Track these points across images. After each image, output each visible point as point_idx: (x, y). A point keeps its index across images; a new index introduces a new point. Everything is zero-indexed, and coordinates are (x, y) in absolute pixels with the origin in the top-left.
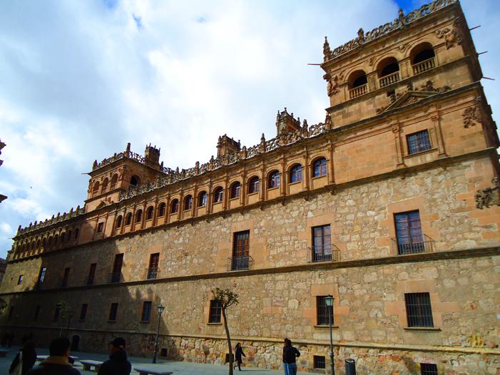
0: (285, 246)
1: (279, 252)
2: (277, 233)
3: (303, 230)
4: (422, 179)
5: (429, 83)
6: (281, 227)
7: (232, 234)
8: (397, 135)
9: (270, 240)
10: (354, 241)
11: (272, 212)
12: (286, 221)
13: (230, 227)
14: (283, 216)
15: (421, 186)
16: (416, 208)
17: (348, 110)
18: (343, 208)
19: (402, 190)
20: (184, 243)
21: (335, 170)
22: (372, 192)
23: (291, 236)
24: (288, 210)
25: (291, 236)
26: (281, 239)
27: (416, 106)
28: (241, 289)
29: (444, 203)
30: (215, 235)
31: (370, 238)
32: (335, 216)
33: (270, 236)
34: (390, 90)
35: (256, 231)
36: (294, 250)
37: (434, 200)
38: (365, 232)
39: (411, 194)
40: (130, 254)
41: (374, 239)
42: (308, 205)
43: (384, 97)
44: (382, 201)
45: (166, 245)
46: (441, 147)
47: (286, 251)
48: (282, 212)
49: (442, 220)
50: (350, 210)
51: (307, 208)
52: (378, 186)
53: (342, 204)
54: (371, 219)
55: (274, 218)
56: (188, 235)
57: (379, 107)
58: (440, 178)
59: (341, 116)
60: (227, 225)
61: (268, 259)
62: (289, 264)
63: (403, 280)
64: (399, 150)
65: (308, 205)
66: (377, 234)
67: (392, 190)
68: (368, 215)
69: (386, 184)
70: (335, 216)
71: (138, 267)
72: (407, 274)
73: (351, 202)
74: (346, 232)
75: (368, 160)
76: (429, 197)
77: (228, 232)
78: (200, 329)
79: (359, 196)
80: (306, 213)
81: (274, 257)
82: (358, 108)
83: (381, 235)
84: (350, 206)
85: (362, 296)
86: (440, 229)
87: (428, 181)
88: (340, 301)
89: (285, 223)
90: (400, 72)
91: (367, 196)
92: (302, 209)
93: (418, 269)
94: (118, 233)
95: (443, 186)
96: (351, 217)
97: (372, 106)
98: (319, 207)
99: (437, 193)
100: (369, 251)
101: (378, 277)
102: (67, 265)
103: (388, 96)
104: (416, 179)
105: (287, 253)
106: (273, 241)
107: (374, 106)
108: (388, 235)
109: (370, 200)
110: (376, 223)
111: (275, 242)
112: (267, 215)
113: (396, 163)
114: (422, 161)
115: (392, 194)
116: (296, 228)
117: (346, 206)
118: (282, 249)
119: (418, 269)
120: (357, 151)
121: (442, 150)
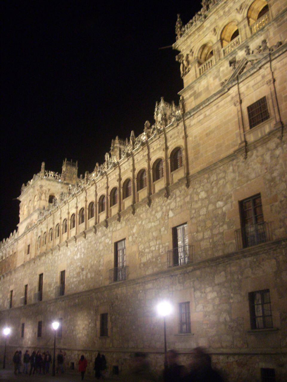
0: (152, 252)
1: (148, 258)
2: (146, 238)
3: (166, 232)
4: (262, 156)
5: (264, 42)
6: (149, 231)
7: (113, 245)
8: (239, 109)
9: (141, 247)
10: (207, 239)
11: (141, 216)
12: (153, 224)
13: (112, 237)
14: (150, 219)
15: (262, 164)
16: (258, 192)
17: (198, 89)
18: (196, 202)
19: (245, 173)
20: (81, 259)
21: (190, 159)
22: (220, 179)
23: (156, 240)
24: (154, 212)
25: (156, 240)
26: (149, 245)
27: (252, 72)
28: (121, 301)
29: (282, 181)
30: (101, 248)
31: (219, 233)
32: (191, 212)
33: (140, 242)
34: (231, 58)
35: (130, 239)
36: (160, 255)
37: (273, 179)
38: (216, 226)
39: (253, 175)
40: (47, 273)
41: (222, 233)
42: (169, 204)
43: (227, 68)
44: (229, 189)
45: (69, 261)
46: (277, 115)
47: (153, 257)
48: (149, 215)
49: (281, 202)
50: (202, 204)
51: (168, 207)
52: (225, 172)
53: (196, 199)
54: (220, 212)
55: (143, 223)
56: (83, 250)
57: (223, 80)
58: (278, 152)
59: (193, 98)
60: (110, 235)
61: (140, 268)
62: (156, 270)
63: (247, 277)
64: (241, 127)
65: (169, 204)
66: (225, 227)
67: (237, 174)
68: (218, 206)
69: (231, 168)
70: (191, 212)
71: (53, 285)
72: (250, 270)
73: (203, 195)
74: (200, 229)
75: (216, 144)
76: (268, 177)
77: (110, 242)
78: (94, 343)
79: (209, 185)
80: (167, 212)
81: (144, 265)
82: (206, 86)
83: (229, 227)
84: (202, 200)
85: (213, 299)
86: (279, 212)
87: (267, 158)
88: (196, 307)
89: (151, 227)
90: (239, 36)
91: (217, 184)
92: (164, 208)
93: (260, 263)
94: (38, 253)
95: (281, 161)
96: (203, 211)
97: (217, 80)
98: (177, 204)
99: (276, 170)
100: (219, 248)
101: (226, 277)
102: (12, 288)
103: (230, 66)
104: (257, 156)
105: (154, 260)
106: (143, 247)
107: (220, 80)
108: (234, 228)
109: (219, 189)
110: (224, 214)
111: (144, 249)
112: (138, 220)
113: (239, 142)
114: (261, 133)
115: (237, 179)
116: (160, 231)
117: (199, 199)
118: (149, 256)
119: (260, 263)
120: (207, 135)
121: (278, 118)
